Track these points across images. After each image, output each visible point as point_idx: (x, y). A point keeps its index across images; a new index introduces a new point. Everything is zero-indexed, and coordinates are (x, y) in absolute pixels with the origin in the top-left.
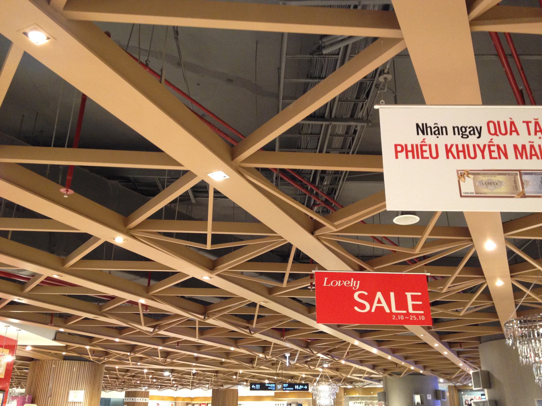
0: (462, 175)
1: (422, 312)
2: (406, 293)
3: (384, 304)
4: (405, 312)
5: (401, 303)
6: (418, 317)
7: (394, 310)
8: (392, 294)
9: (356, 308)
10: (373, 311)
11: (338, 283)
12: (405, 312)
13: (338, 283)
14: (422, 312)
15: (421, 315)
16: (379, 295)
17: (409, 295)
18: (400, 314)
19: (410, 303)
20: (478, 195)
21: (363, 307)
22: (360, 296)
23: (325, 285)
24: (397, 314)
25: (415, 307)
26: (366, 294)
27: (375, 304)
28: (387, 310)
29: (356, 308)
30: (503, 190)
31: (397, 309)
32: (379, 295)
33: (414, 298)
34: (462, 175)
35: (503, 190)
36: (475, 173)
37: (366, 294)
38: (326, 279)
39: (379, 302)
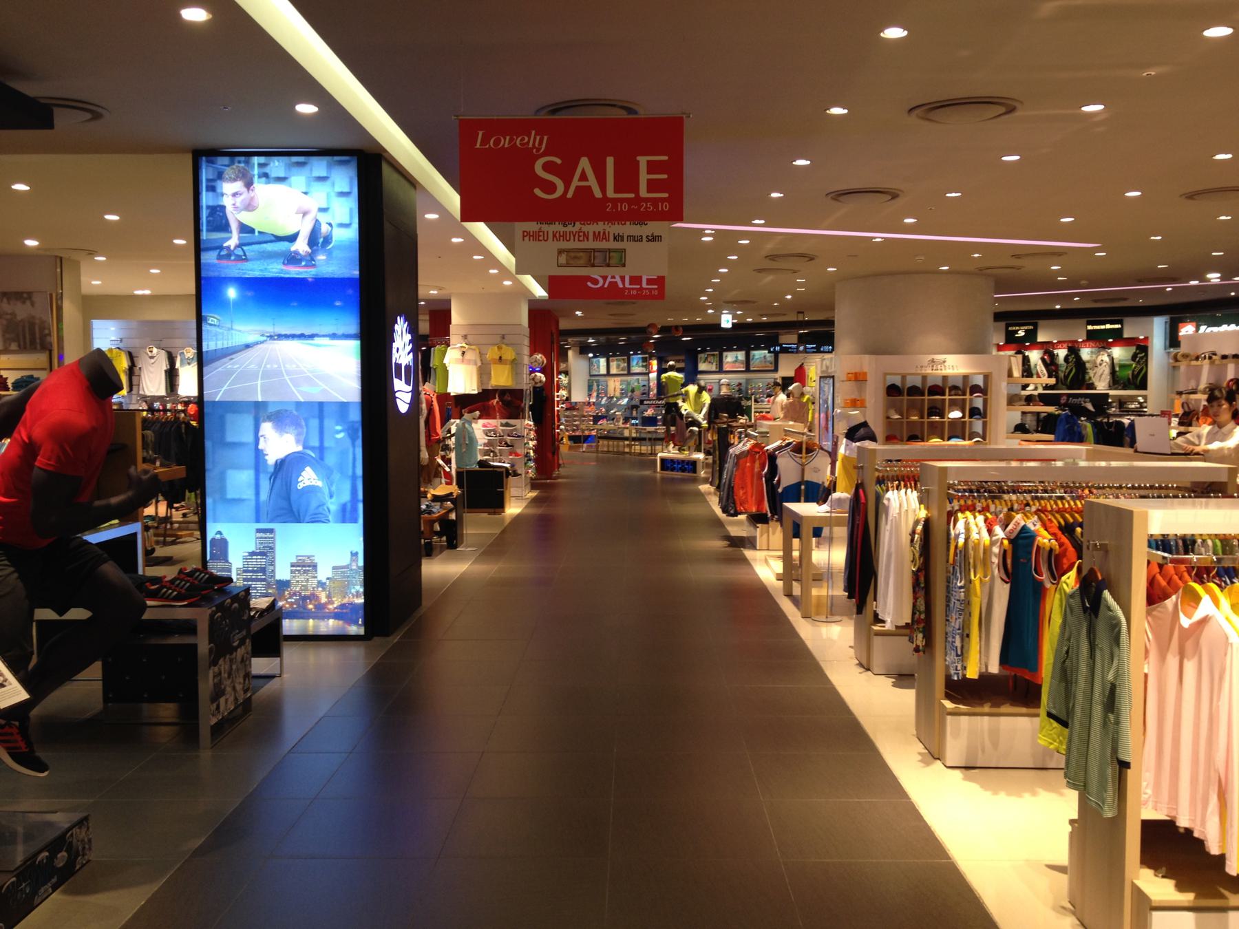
0: (560, 252)
1: (665, 195)
2: (639, 158)
3: (592, 182)
4: (632, 195)
5: (627, 179)
6: (656, 206)
7: (611, 193)
8: (610, 161)
9: (538, 192)
10: (570, 195)
11: (505, 142)
12: (632, 195)
13: (505, 142)
14: (665, 195)
15: (662, 200)
16: (584, 163)
17: (643, 161)
18: (622, 200)
19: (644, 177)
20: (567, 265)
21: (550, 188)
22: (548, 167)
23: (478, 146)
24: (615, 201)
25: (652, 186)
26: (559, 161)
27: (576, 182)
28: (598, 193)
29: (538, 192)
30: (582, 262)
31: (616, 191)
32: (584, 163)
33: (652, 168)
34: (560, 252)
35: (582, 262)
36: (568, 251)
37: (559, 161)
38: (481, 133)
39: (584, 177)
